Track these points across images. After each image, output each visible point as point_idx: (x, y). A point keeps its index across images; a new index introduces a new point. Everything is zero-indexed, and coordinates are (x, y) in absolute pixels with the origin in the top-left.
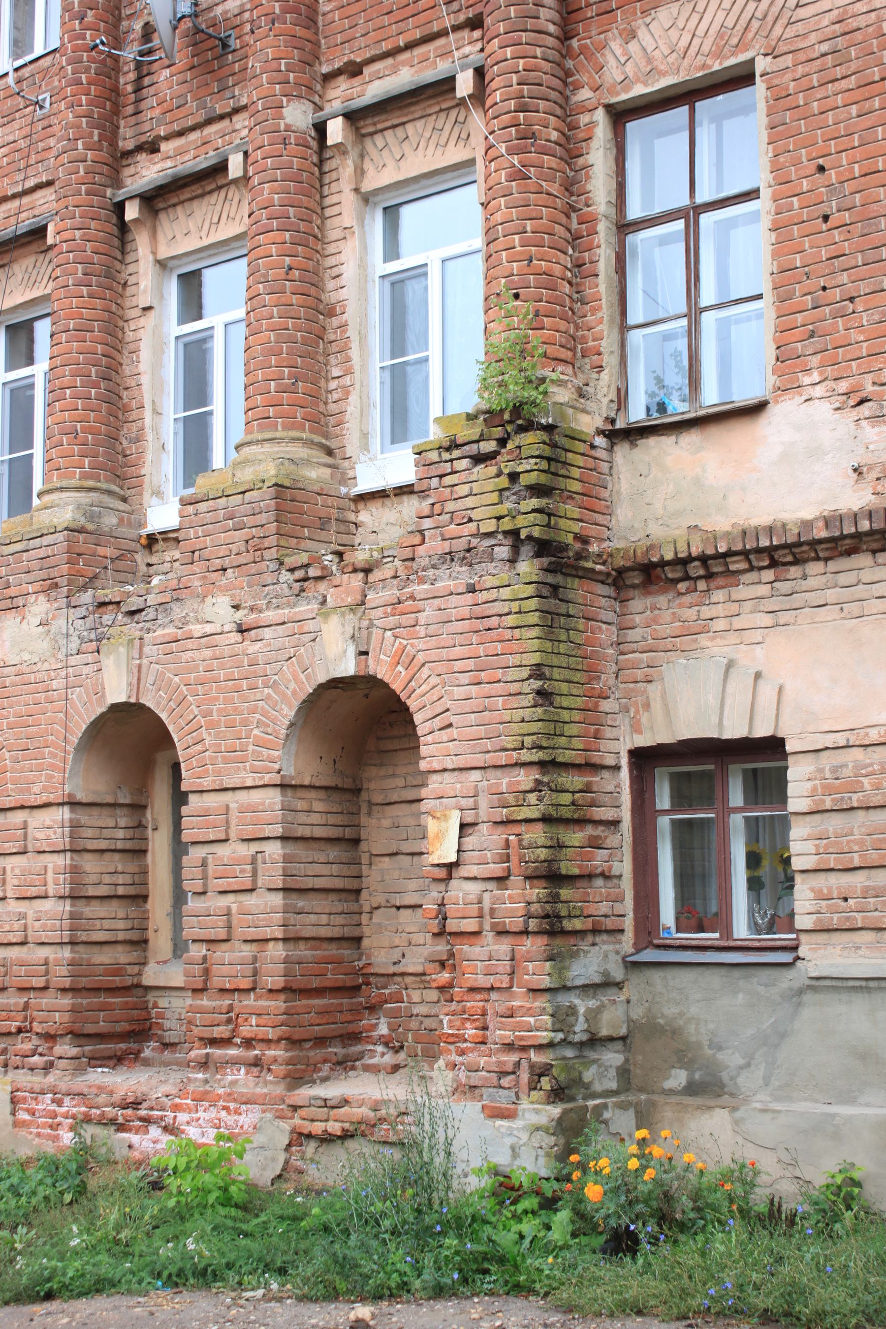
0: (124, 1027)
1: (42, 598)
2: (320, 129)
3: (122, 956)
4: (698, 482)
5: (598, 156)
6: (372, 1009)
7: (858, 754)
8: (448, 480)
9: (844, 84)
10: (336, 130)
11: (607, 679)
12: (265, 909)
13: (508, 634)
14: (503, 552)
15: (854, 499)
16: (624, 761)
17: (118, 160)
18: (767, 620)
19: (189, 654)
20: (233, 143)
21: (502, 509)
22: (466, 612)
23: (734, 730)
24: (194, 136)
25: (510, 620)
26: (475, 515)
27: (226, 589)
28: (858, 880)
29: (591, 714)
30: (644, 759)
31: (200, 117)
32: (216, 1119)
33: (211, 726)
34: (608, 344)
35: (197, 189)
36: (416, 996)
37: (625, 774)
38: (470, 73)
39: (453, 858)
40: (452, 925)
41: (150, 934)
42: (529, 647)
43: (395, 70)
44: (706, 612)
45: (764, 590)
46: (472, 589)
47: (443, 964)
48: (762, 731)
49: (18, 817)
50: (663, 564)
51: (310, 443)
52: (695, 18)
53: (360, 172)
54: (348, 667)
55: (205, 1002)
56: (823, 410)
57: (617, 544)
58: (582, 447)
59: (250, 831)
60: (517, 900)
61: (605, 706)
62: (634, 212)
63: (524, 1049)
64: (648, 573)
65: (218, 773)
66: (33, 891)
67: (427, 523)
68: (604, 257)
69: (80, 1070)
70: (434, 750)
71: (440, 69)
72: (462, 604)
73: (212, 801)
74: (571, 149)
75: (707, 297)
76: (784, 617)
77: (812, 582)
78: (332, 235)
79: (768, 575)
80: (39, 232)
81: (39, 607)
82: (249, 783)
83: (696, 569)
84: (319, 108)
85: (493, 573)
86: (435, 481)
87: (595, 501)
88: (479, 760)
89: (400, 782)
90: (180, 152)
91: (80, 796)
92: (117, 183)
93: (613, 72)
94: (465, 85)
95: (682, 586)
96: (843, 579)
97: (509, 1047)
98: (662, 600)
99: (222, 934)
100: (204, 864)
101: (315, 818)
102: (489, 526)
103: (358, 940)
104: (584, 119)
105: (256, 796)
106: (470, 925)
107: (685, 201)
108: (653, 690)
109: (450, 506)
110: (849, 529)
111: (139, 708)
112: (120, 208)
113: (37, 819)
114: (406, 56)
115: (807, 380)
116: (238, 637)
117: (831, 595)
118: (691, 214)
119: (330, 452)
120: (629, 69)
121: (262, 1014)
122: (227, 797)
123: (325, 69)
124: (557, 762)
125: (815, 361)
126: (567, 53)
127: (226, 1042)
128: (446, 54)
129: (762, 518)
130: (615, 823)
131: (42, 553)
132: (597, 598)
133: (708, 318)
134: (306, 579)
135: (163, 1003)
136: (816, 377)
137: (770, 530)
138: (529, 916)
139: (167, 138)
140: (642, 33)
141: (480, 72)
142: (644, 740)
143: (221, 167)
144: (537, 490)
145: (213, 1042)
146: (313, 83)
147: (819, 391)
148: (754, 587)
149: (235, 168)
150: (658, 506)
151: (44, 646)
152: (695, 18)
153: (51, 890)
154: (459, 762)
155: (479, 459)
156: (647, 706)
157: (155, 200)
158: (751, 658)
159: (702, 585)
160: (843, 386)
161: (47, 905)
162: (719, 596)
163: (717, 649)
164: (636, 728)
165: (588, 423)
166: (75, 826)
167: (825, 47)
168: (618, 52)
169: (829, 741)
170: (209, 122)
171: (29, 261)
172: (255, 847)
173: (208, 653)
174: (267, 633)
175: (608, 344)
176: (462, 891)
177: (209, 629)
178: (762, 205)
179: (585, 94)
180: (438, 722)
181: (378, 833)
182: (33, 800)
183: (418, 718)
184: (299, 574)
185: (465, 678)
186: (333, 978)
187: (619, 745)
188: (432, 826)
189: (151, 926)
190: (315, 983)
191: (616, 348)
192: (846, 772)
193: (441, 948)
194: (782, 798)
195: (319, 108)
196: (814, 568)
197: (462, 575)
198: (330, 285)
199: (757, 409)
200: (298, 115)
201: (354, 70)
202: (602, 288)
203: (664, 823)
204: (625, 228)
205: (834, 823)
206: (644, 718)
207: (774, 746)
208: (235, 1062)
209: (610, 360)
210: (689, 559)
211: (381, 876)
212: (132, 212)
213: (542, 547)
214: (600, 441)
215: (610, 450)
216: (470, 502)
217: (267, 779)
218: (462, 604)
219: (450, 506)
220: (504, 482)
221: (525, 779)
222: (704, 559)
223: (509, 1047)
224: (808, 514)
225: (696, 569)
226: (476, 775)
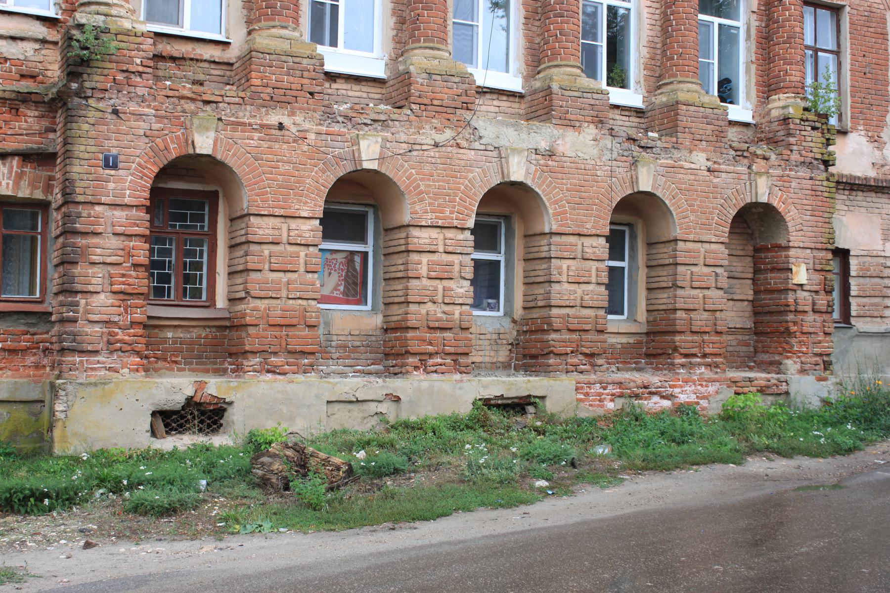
1: (592, 126)
7: (869, 258)
8: (803, 133)
13: (825, 199)
15: (872, 174)
19: (681, 176)
22: (809, 187)
25: (826, 194)
26: (815, 150)
27: (703, 150)
28: (866, 300)
32: (698, 390)
45: (845, 197)
46: (811, 178)
49: (572, 239)
56: (864, 140)
76: (852, 208)
77: (859, 198)
79: (847, 192)
82: (713, 240)
88: (812, 245)
96: (869, 199)
97: (816, 355)
102: (819, 156)
105: (713, 246)
109: (804, 144)
110: (880, 184)
116: (708, 173)
117: (864, 204)
125: (862, 122)
127: (695, 355)
131: (593, 102)
136: (861, 128)
147: (862, 133)
151: (595, 152)
153: (594, 280)
154: (806, 245)
160: (870, 134)
161: (590, 287)
167: (866, 14)
169: (862, 253)
173: (692, 177)
174: (724, 175)
177: (693, 166)
182: (585, 232)
183: (789, 224)
184: (739, 153)
185: (808, 213)
192: (867, 264)
196: (860, 193)
197: (803, 172)
205: (862, 280)
208: (699, 364)
216: (811, 144)
223: (816, 355)
224: (859, 174)
226: (809, 251)
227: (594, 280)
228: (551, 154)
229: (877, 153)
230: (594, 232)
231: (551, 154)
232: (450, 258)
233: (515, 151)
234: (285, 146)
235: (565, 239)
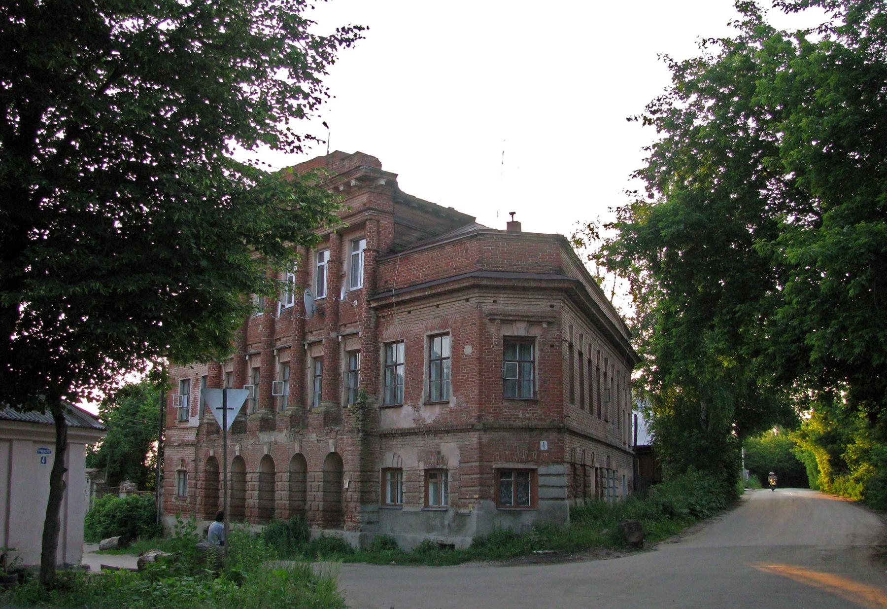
3: (300, 503)
15: (413, 425)
23: (395, 466)
30: (385, 470)
53: (345, 347)
56: (410, 408)
60: (356, 496)
68: (382, 372)
73: (313, 474)
74: (377, 350)
81: (285, 431)
87: (376, 420)
93: (384, 337)
142: (384, 466)
148: (400, 439)
165: (376, 406)
175: (382, 390)
200: (333, 335)
207: (401, 469)
213: (363, 431)
221: (359, 473)
229: (416, 413)
231: (276, 443)
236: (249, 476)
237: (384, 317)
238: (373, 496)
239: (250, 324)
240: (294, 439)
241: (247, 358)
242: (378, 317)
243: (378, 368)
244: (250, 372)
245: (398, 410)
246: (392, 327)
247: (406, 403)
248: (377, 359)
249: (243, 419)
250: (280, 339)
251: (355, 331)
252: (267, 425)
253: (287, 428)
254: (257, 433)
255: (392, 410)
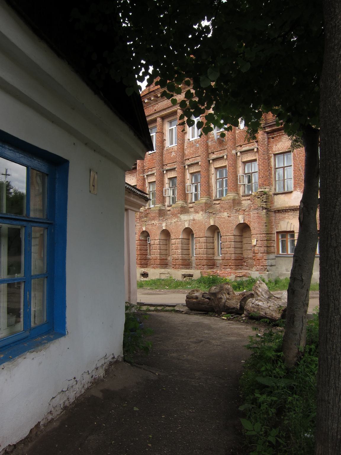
0: (212, 264)
1: (201, 212)
2: (237, 153)
3: (212, 255)
4: (284, 201)
5: (272, 160)
6: (244, 262)
8: (254, 200)
9: (302, 154)
10: (239, 154)
11: (273, 223)
12: (232, 250)
14: (261, 209)
16: (275, 233)
17: (208, 154)
18: (292, 217)
19: (222, 219)
20: (224, 154)
21: (261, 204)
23: (288, 230)
24: (219, 152)
29: (271, 228)
30: (277, 232)
31: (220, 150)
33: (224, 228)
34: (274, 183)
35: (220, 159)
36: (250, 260)
37: (276, 234)
38: (256, 149)
39: (255, 244)
40: (255, 252)
41: (215, 253)
42: (265, 220)
43: (246, 146)
44: (285, 216)
45: (292, 214)
46: (257, 213)
47: (254, 256)
48: (292, 230)
49: (199, 238)
50: (280, 210)
51: (236, 193)
52: (284, 144)
53: (242, 159)
54: (242, 222)
55: (224, 261)
57: (274, 208)
58: (270, 196)
59: (230, 241)
60: (262, 249)
61: (273, 226)
62: (277, 167)
63: (264, 266)
64: (279, 211)
65: (225, 234)
66: (201, 248)
67: (252, 205)
68: (273, 172)
69: (208, 270)
70: (253, 232)
71: (252, 147)
72: (256, 215)
74: (269, 159)
75: (286, 178)
78: (238, 167)
79: (293, 212)
80: (198, 163)
81: (201, 213)
83: (284, 211)
84: (236, 151)
85: (260, 211)
86: (253, 200)
87: (272, 202)
88: (258, 233)
89: (248, 235)
90: (217, 154)
91: (207, 236)
92: (208, 158)
93: (274, 150)
94: (255, 150)
95: (282, 213)
97: (262, 266)
98: (280, 214)
99: (226, 253)
100: (224, 244)
101: (237, 239)
103: (242, 254)
104: (270, 155)
106: (257, 252)
107: (283, 166)
108: (279, 225)
109: (255, 203)
111: (215, 225)
112: (209, 161)
113: (201, 239)
114: (247, 145)
115: (297, 189)
116: (228, 217)
118: (284, 167)
119: (238, 194)
120: (276, 149)
121: (232, 262)
122: (227, 237)
123: (237, 145)
124: (269, 233)
125: (298, 187)
126: (269, 147)
127: (227, 266)
128: (253, 145)
129: (292, 205)
130: (274, 240)
131: (201, 206)
132: (273, 214)
133: (286, 180)
134: (237, 211)
135: (217, 261)
136: (298, 189)
137: (293, 207)
138: (264, 251)
139: (215, 152)
140: (278, 145)
141: (257, 149)
142: (278, 231)
143: (223, 157)
144: (265, 202)
145: (225, 266)
146: (235, 149)
147: (299, 191)
149: (225, 157)
150: (280, 203)
151: (202, 218)
152: (284, 144)
153: (203, 247)
155: (259, 198)
156: (278, 227)
157: (214, 160)
158: (291, 221)
159: (285, 213)
161: (203, 249)
162: (287, 214)
163: (287, 221)
164: (277, 229)
165: (271, 193)
166: (206, 240)
168: (275, 147)
170: (221, 150)
171: (196, 166)
172: (230, 243)
173: (224, 219)
174: (232, 217)
175: (274, 183)
176: (256, 248)
177: (224, 216)
178: (292, 167)
179: (271, 152)
180: (253, 229)
181: (245, 241)
182: (201, 236)
183: (251, 228)
184: (236, 210)
185: (257, 223)
186: (240, 258)
187: (275, 231)
188: (253, 240)
189: (215, 252)
190: (238, 259)
191: (275, 183)
193: (254, 255)
194: (294, 238)
195: (236, 151)
197: (256, 212)
198: (238, 173)
199: (291, 192)
200: (234, 152)
201: (241, 146)
202: (273, 176)
203: (280, 240)
204: (276, 169)
206: (278, 228)
207: (293, 232)
208: (229, 268)
209: (274, 185)
210: (283, 210)
211: (245, 246)
212: (211, 162)
214: (272, 195)
215: (274, 196)
216: (257, 203)
217: (232, 235)
218: (256, 215)
219: (255, 203)
220: (261, 201)
222: (285, 210)
223: (262, 266)
225: (284, 211)
226: (258, 235)
227: (203, 247)
228: (194, 220)
230: (202, 236)
231: (194, 220)
232: (178, 245)
233: (186, 220)
234: (154, 227)
235: (197, 238)
236: (173, 241)
237: (273, 138)
238: (272, 249)
239: (165, 152)
240: (209, 218)
241: (165, 172)
242: (268, 138)
243: (270, 170)
244: (166, 181)
245: (289, 195)
246: (280, 143)
247: (295, 190)
248: (269, 164)
249: (164, 208)
250: (188, 159)
251: (221, 155)
252: (184, 210)
253: (202, 210)
254: (179, 215)
255: (283, 195)
